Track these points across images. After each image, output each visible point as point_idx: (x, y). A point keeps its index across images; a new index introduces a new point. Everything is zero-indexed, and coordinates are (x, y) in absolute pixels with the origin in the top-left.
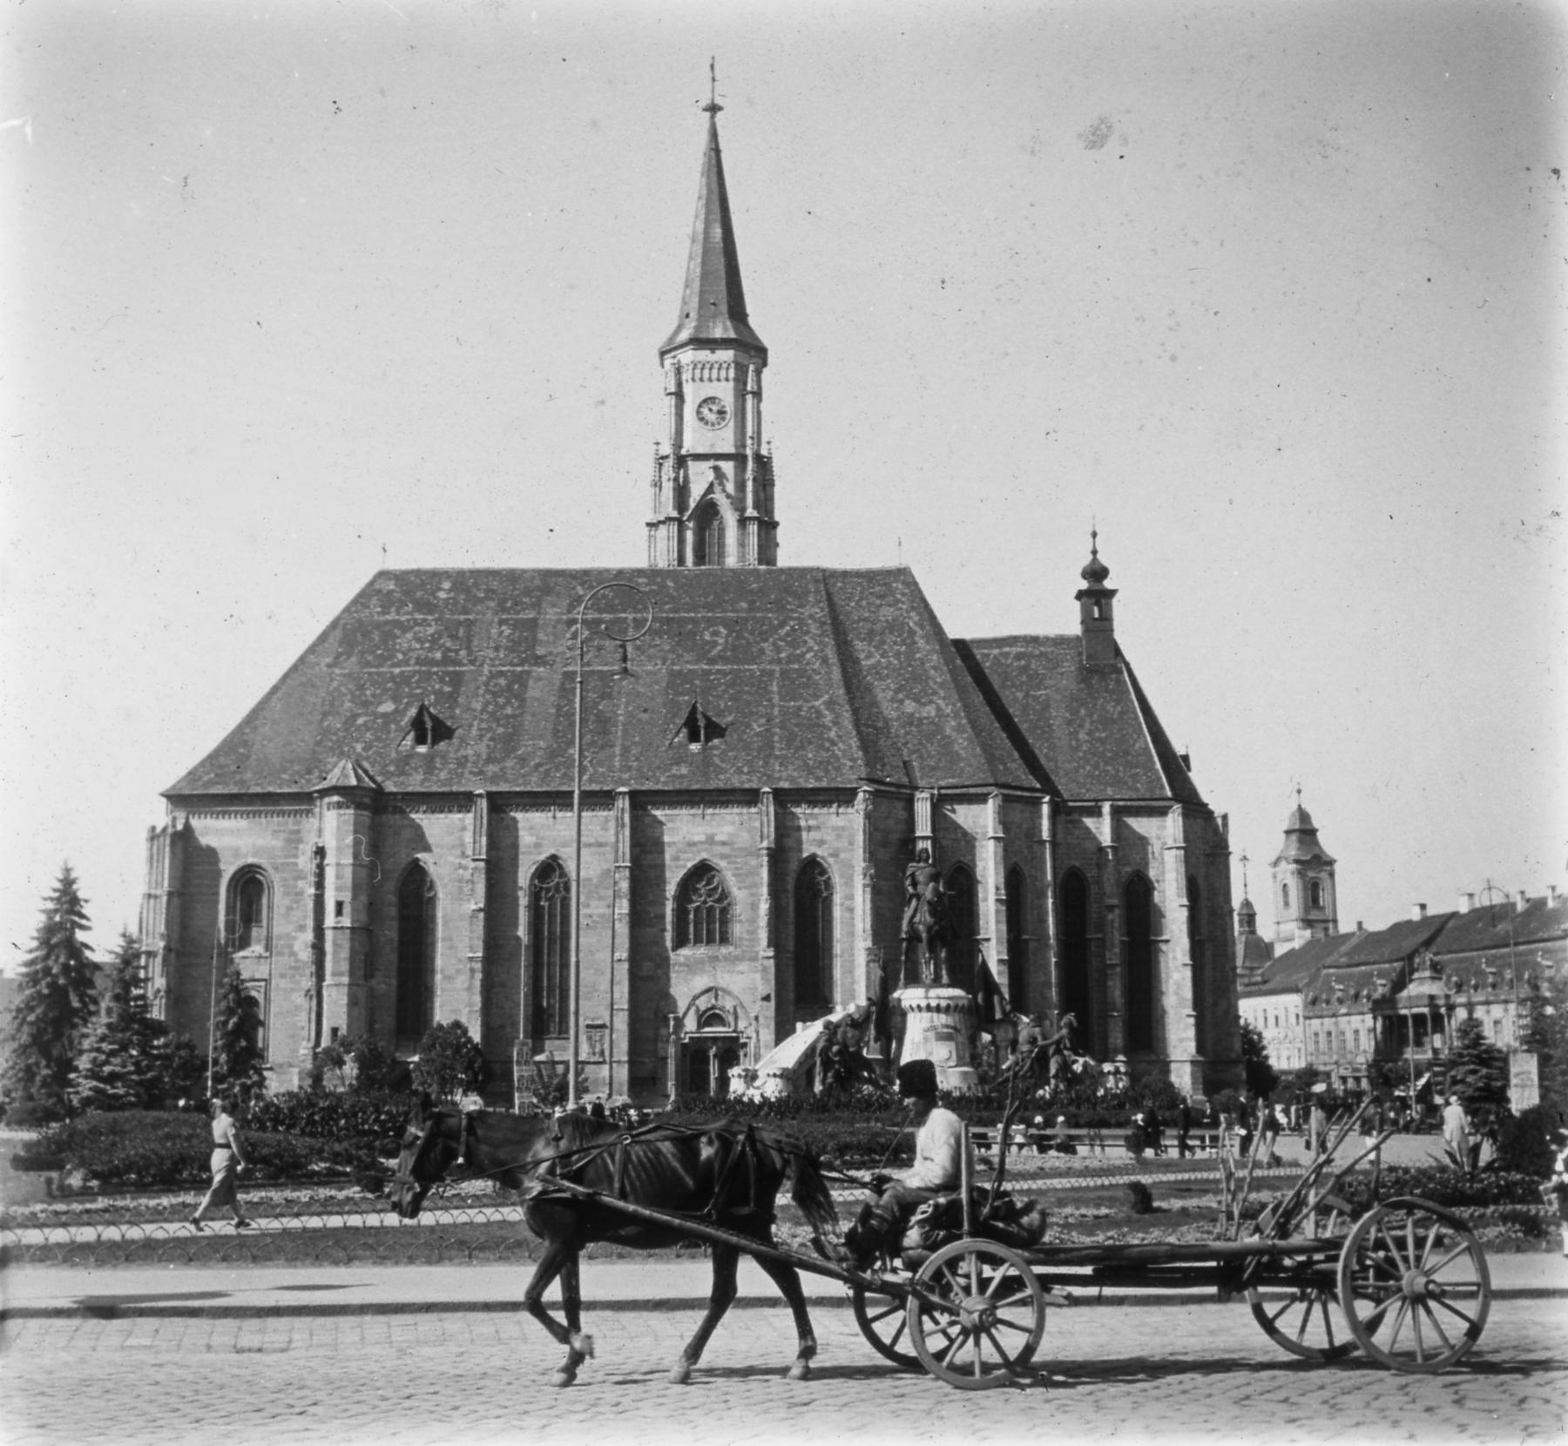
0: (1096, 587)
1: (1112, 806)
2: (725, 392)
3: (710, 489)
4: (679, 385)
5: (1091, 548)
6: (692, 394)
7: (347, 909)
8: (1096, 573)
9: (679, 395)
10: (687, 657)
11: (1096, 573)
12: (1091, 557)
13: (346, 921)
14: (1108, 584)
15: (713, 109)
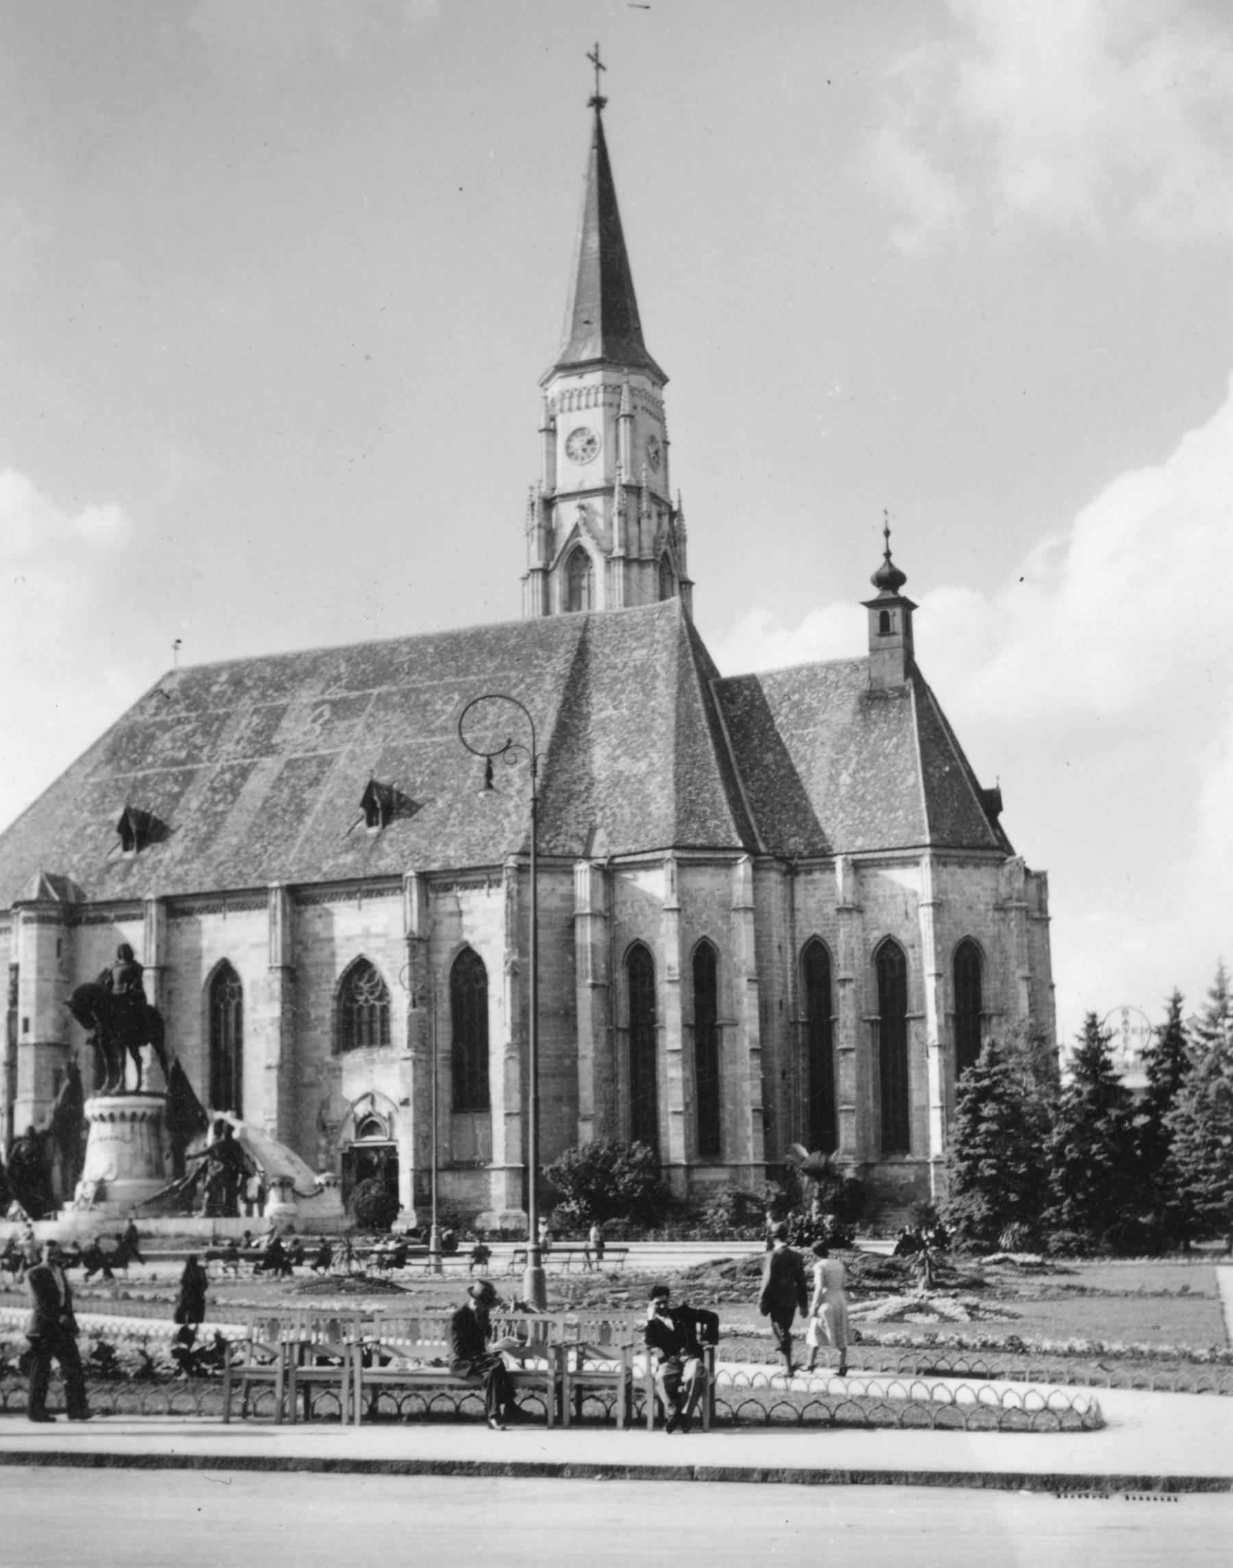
0: (890, 595)
1: (845, 860)
2: (594, 419)
3: (576, 531)
4: (553, 419)
5: (884, 550)
6: (565, 424)
7: (32, 1026)
8: (890, 579)
9: (551, 432)
10: (410, 731)
11: (890, 579)
12: (883, 560)
13: (31, 1038)
14: (903, 591)
15: (598, 103)
